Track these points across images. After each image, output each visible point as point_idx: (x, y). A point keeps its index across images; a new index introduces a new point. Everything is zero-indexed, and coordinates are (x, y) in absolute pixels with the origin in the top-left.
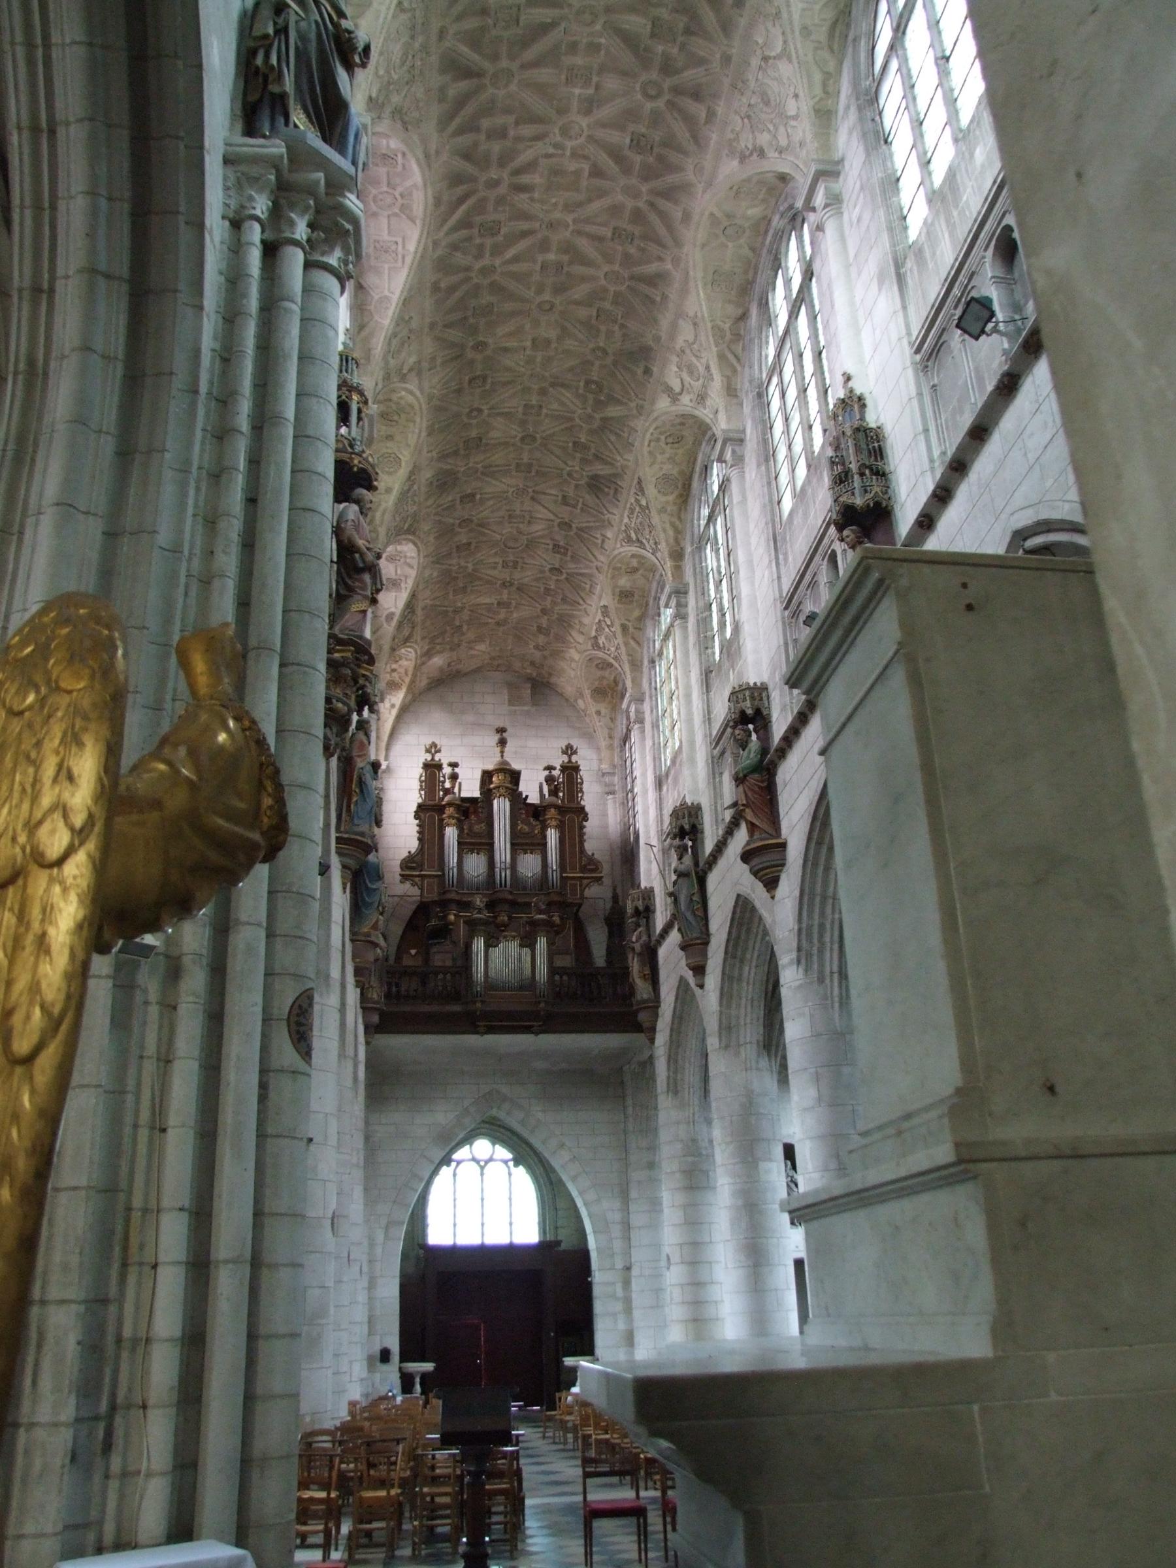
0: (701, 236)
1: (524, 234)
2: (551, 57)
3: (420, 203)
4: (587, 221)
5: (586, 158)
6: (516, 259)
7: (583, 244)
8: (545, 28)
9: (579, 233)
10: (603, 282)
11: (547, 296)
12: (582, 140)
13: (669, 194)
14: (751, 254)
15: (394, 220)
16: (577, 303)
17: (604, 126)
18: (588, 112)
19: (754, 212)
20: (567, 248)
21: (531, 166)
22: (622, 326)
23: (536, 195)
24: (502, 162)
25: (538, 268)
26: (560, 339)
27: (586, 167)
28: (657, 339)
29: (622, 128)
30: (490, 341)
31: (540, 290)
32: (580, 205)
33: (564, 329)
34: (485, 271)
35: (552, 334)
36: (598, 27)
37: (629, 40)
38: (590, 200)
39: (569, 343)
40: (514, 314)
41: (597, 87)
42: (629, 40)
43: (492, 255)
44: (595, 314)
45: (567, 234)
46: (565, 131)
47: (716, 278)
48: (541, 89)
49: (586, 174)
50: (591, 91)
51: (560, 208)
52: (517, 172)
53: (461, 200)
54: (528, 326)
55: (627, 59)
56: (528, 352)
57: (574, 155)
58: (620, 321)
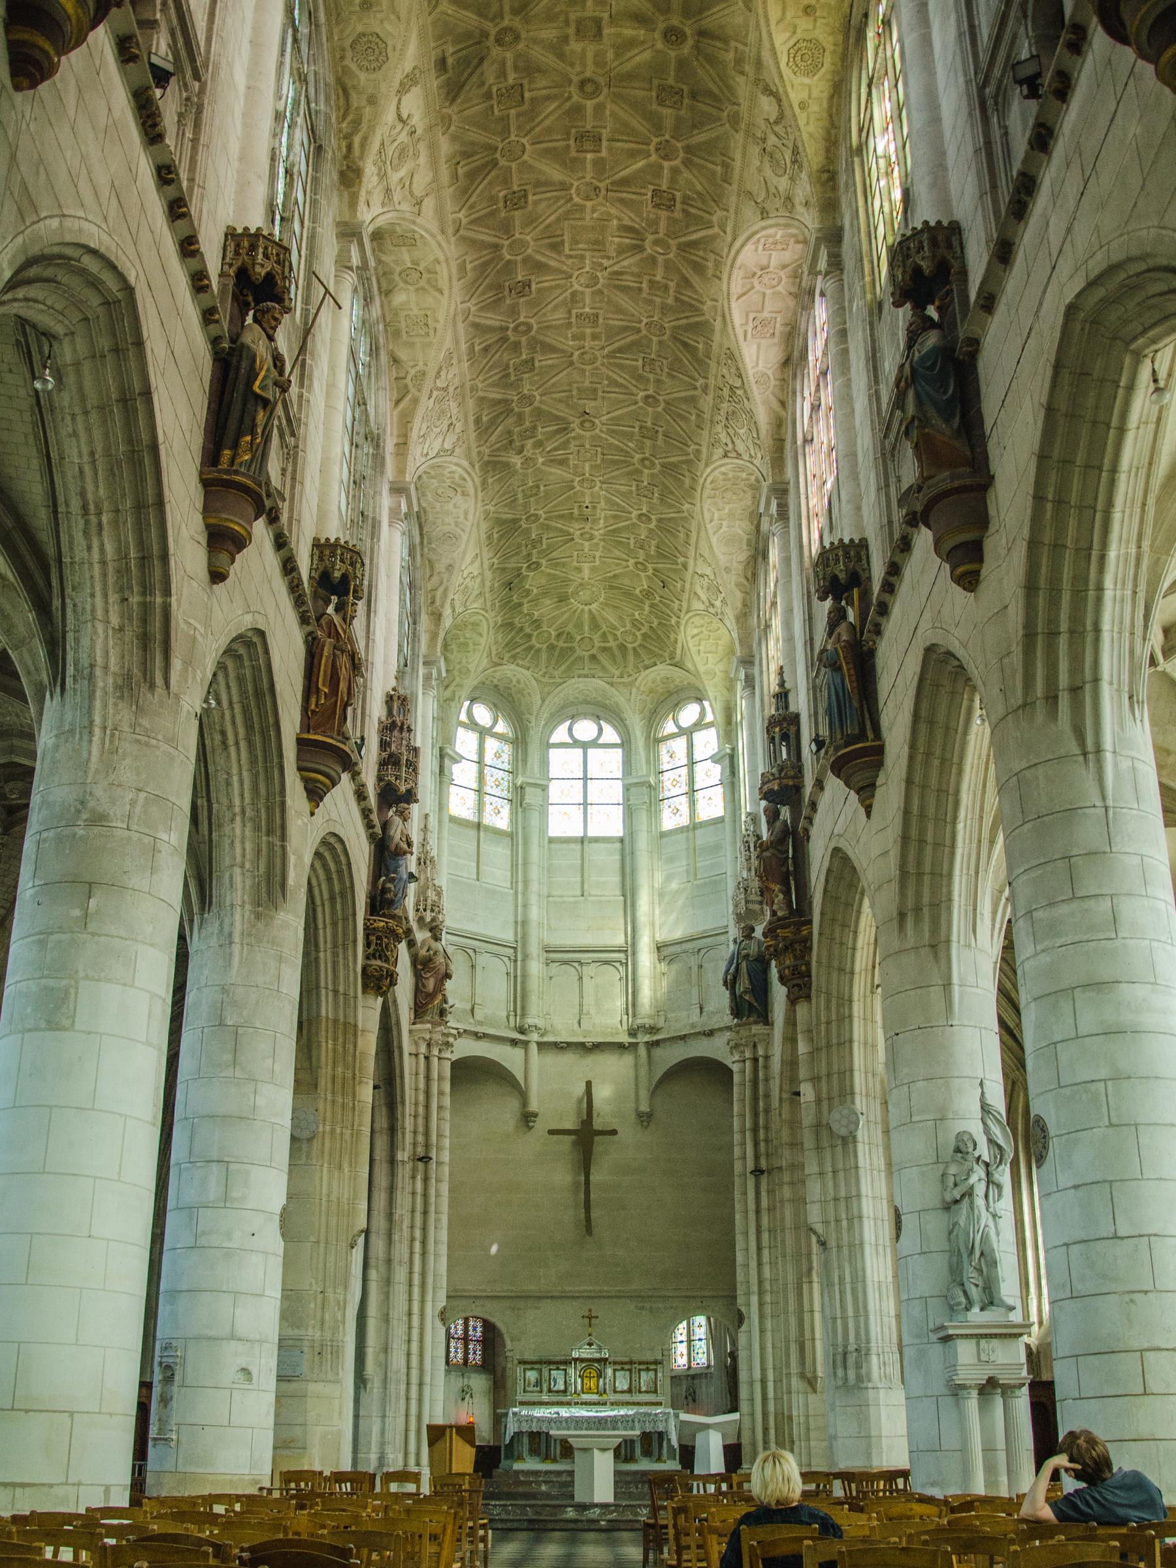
0: (443, 270)
1: (625, 182)
2: (611, 332)
3: (737, 285)
4: (557, 199)
5: (570, 257)
6: (633, 155)
7: (555, 173)
8: (620, 350)
9: (564, 187)
10: (524, 141)
11: (590, 104)
12: (576, 274)
13: (485, 265)
14: (384, 258)
15: (764, 262)
16: (548, 98)
17: (557, 287)
18: (574, 294)
19: (399, 298)
20: (573, 165)
21: (621, 250)
22: (488, 96)
23: (615, 222)
24: (653, 260)
25: (605, 143)
26: (565, 39)
27: (567, 251)
28: (446, 121)
29: (539, 290)
30: (659, 45)
31: (599, 108)
32: (566, 216)
33: (561, 56)
34: (665, 152)
35: (575, 46)
36: (577, 353)
37: (549, 348)
38: (558, 220)
39: (549, 33)
40: (630, 76)
41: (569, 312)
42: (549, 348)
43: (662, 167)
44: (527, 95)
45: (576, 184)
46: (594, 280)
47: (409, 240)
48: (619, 310)
49: (567, 245)
50: (574, 312)
51: (588, 210)
52: (639, 248)
53: (693, 244)
54: (610, 55)
55: (551, 339)
56: (606, 16)
57: (582, 257)
58: (494, 102)
